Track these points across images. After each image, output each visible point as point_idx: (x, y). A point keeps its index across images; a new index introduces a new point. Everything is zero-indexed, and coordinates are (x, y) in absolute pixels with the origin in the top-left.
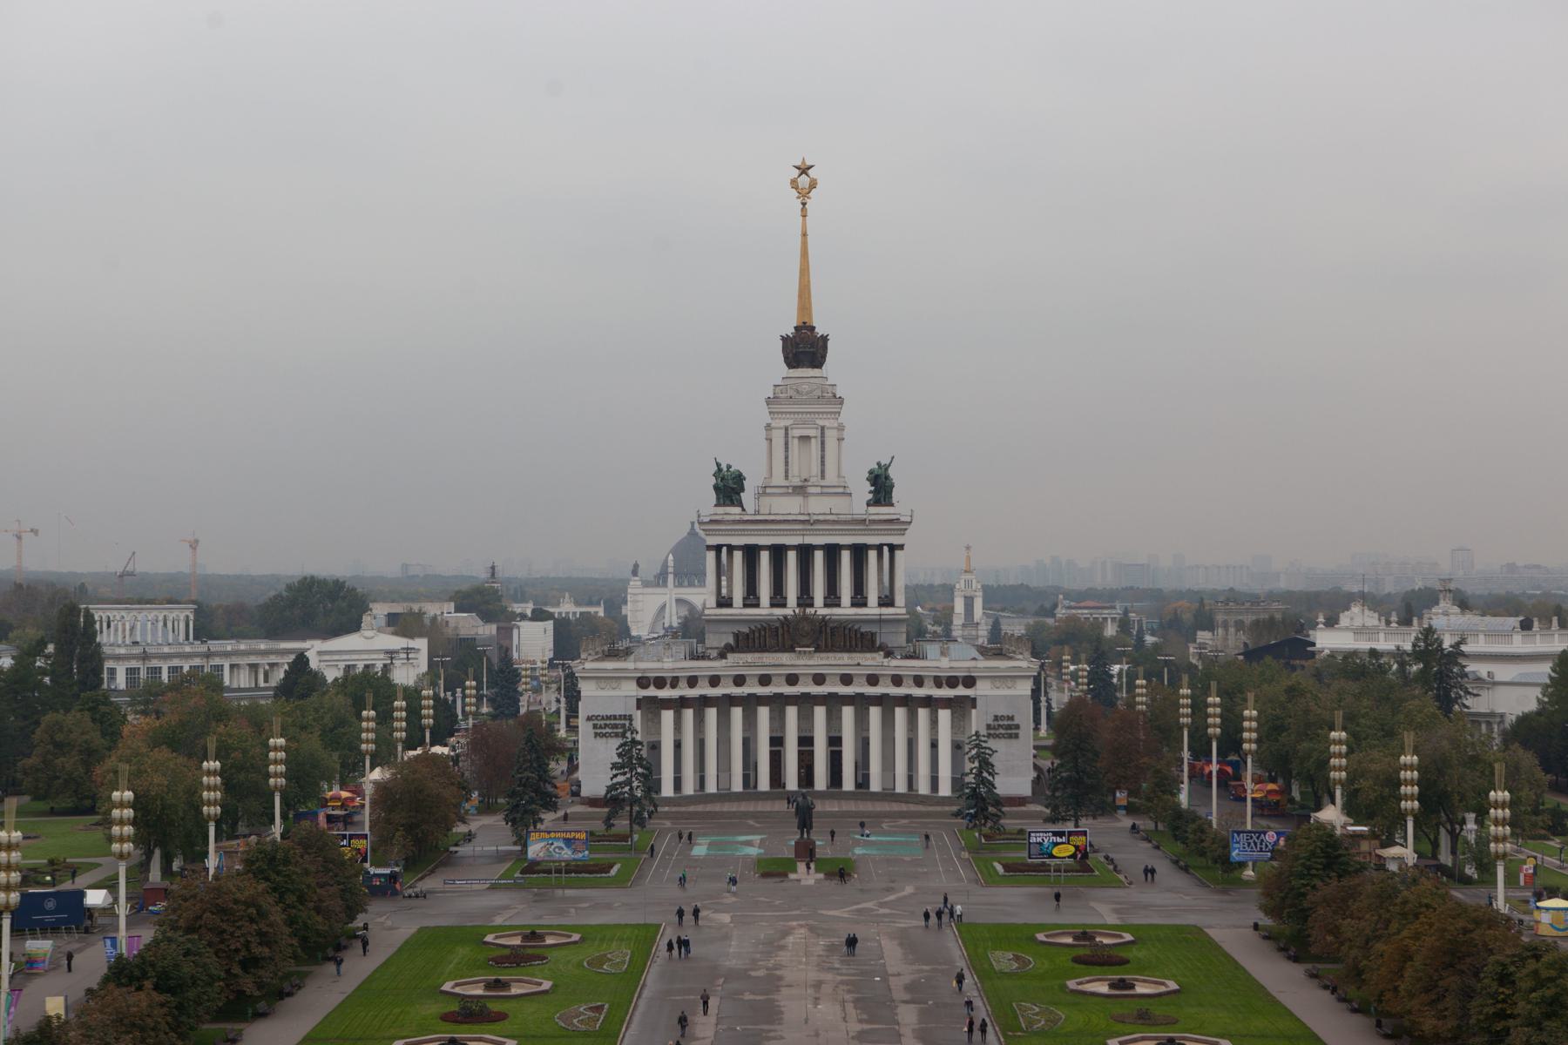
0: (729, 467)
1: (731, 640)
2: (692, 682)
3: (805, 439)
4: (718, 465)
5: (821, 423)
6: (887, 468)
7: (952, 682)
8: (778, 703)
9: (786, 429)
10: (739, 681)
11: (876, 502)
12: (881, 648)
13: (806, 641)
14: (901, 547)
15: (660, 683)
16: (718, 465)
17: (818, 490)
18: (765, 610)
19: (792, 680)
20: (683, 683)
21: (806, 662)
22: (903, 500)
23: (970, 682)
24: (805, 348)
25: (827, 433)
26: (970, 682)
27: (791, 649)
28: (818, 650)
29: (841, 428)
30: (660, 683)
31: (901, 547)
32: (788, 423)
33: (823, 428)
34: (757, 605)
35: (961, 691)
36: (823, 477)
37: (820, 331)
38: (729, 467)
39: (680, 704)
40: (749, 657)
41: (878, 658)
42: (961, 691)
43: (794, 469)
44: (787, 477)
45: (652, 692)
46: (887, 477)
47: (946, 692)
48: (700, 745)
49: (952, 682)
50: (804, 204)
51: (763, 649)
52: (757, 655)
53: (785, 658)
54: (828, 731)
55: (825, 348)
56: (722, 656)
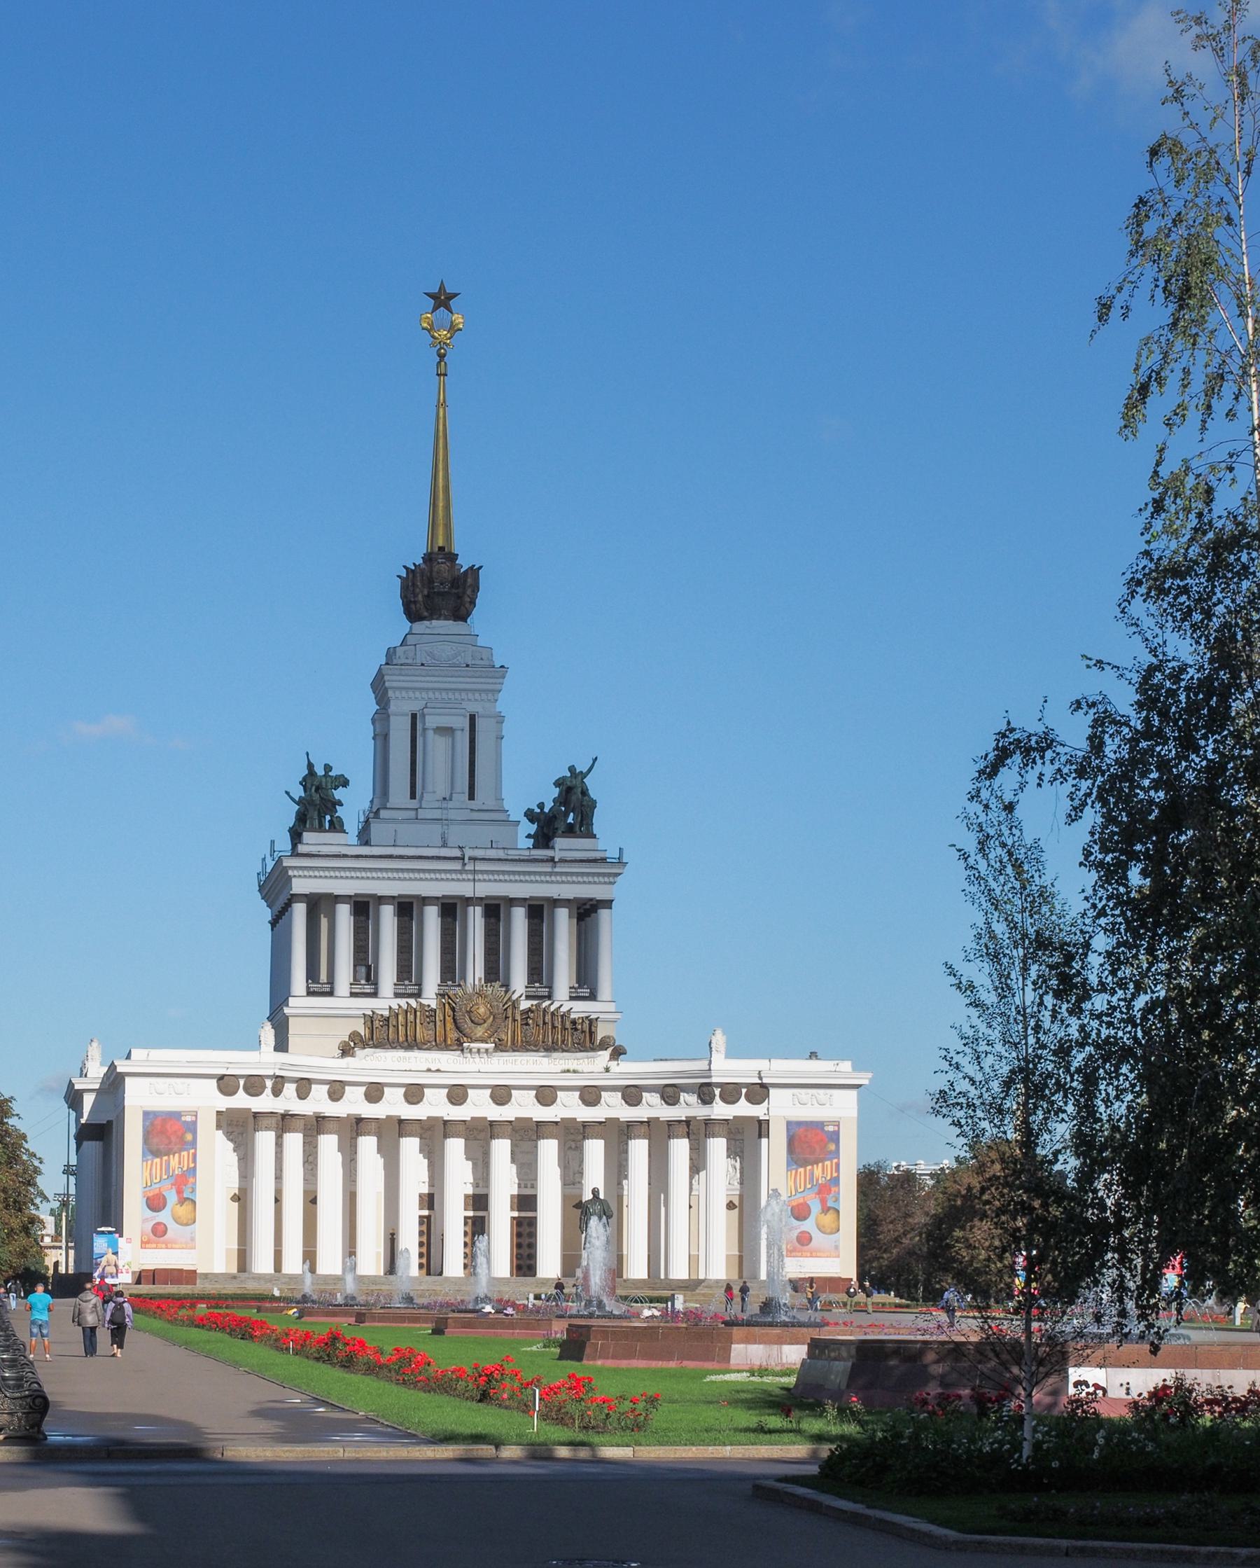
0: (328, 768)
3: (448, 731)
5: (473, 707)
6: (584, 775)
7: (731, 1093)
8: (434, 1134)
9: (414, 716)
10: (374, 1092)
11: (570, 831)
12: (603, 1045)
13: (480, 1031)
14: (608, 904)
15: (254, 1085)
17: (467, 815)
18: (386, 1002)
19: (457, 1095)
20: (290, 1089)
21: (481, 1066)
23: (759, 1092)
24: (439, 590)
25: (480, 723)
26: (759, 1092)
27: (459, 1046)
28: (500, 1047)
29: (500, 719)
30: (254, 1085)
31: (608, 904)
32: (415, 707)
33: (472, 718)
34: (374, 994)
35: (743, 1108)
36: (472, 796)
37: (464, 563)
38: (328, 768)
39: (284, 1122)
42: (743, 1108)
44: (413, 796)
45: (241, 1100)
46: (585, 793)
47: (720, 1110)
48: (311, 1200)
49: (731, 1093)
51: (411, 1044)
52: (401, 1053)
55: (476, 588)
56: (346, 1051)
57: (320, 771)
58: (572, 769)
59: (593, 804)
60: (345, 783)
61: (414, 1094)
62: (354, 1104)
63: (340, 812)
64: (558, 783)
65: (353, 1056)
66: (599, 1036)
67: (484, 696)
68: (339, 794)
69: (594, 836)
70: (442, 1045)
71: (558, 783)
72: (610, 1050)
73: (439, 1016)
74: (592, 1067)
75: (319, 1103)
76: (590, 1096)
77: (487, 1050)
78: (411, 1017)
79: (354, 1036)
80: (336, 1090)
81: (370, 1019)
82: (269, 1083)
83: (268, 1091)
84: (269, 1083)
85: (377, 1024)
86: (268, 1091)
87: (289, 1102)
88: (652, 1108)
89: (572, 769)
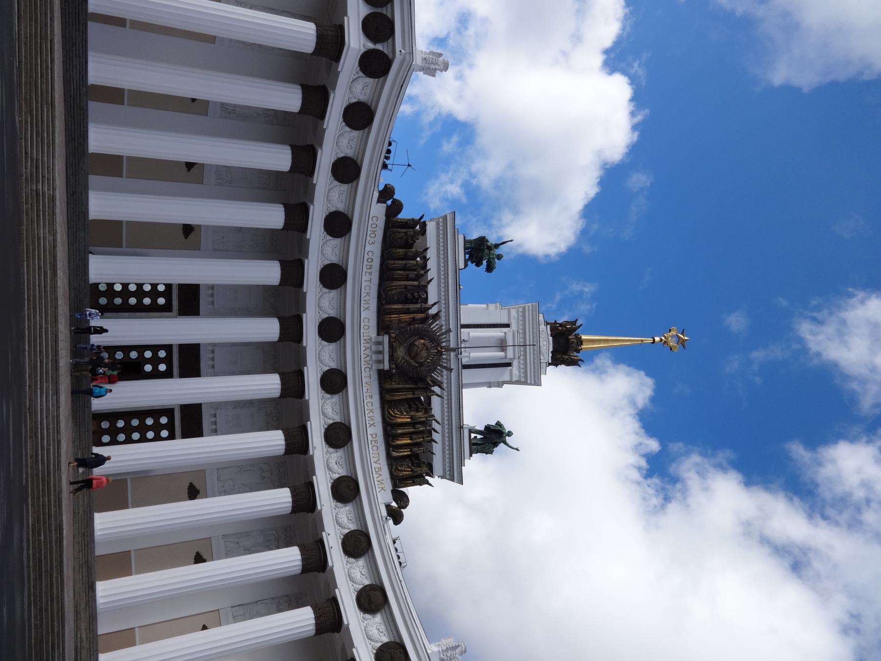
1: (403, 216)
2: (359, 116)
4: (497, 246)
5: (515, 364)
10: (338, 225)
13: (401, 352)
16: (497, 246)
19: (332, 330)
22: (475, 466)
27: (383, 327)
28: (383, 376)
29: (500, 385)
32: (514, 326)
33: (509, 365)
36: (466, 367)
38: (499, 257)
40: (373, 249)
41: (385, 497)
43: (474, 333)
46: (496, 445)
50: (661, 340)
51: (386, 274)
53: (369, 316)
54: (217, 406)
57: (497, 252)
58: (510, 434)
59: (489, 452)
60: (490, 268)
61: (334, 276)
62: (326, 194)
63: (472, 266)
64: (498, 424)
65: (379, 201)
66: (412, 491)
67: (522, 371)
68: (484, 262)
69: (471, 456)
70: (382, 313)
71: (498, 424)
72: (394, 504)
73: (412, 306)
74: (377, 488)
75: (335, 139)
76: (346, 490)
77: (381, 362)
78: (412, 274)
79: (395, 208)
80: (346, 170)
81: (417, 227)
82: (379, 47)
83: (371, 46)
84: (379, 47)
85: (410, 232)
86: (371, 46)
87: (348, 85)
88: (347, 577)
89: (510, 434)
